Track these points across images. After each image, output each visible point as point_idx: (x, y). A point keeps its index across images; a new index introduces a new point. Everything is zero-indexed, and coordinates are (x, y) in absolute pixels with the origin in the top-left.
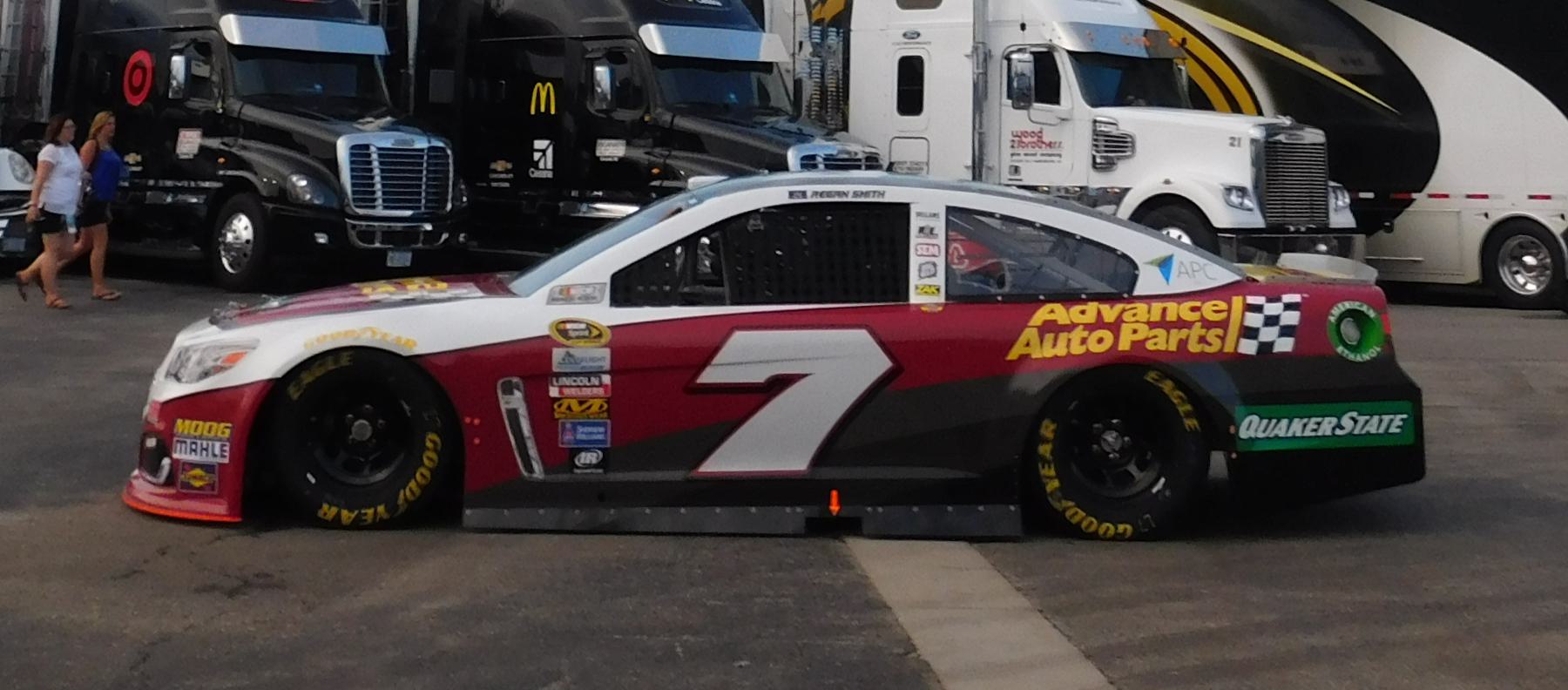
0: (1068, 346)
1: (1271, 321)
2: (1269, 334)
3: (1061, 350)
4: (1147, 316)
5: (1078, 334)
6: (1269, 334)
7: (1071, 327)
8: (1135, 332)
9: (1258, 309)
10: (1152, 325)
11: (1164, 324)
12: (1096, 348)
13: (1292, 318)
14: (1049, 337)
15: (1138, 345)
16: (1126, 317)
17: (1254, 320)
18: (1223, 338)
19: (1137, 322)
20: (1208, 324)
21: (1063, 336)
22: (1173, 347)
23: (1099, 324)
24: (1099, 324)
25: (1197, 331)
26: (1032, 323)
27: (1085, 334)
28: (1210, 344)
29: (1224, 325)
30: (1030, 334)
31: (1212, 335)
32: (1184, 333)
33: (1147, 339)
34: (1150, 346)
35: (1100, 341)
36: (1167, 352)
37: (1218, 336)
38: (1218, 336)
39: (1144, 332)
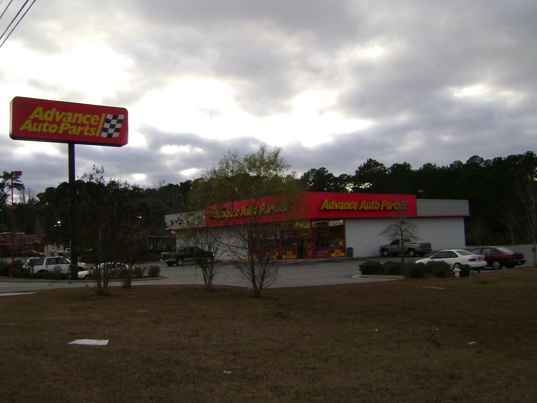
0: (42, 128)
1: (112, 126)
2: (111, 131)
3: (39, 130)
4: (71, 121)
5: (46, 125)
6: (111, 131)
7: (44, 122)
8: (65, 126)
9: (108, 121)
10: (72, 124)
11: (77, 125)
12: (51, 131)
14: (35, 124)
15: (65, 132)
16: (64, 120)
17: (107, 126)
18: (96, 131)
19: (67, 122)
20: (91, 126)
22: (78, 133)
23: (54, 122)
24: (54, 122)
25: (87, 128)
26: (30, 118)
27: (48, 125)
28: (91, 133)
29: (97, 126)
30: (29, 122)
31: (92, 130)
32: (83, 128)
33: (69, 130)
34: (70, 133)
35: (53, 129)
36: (76, 135)
39: (69, 126)
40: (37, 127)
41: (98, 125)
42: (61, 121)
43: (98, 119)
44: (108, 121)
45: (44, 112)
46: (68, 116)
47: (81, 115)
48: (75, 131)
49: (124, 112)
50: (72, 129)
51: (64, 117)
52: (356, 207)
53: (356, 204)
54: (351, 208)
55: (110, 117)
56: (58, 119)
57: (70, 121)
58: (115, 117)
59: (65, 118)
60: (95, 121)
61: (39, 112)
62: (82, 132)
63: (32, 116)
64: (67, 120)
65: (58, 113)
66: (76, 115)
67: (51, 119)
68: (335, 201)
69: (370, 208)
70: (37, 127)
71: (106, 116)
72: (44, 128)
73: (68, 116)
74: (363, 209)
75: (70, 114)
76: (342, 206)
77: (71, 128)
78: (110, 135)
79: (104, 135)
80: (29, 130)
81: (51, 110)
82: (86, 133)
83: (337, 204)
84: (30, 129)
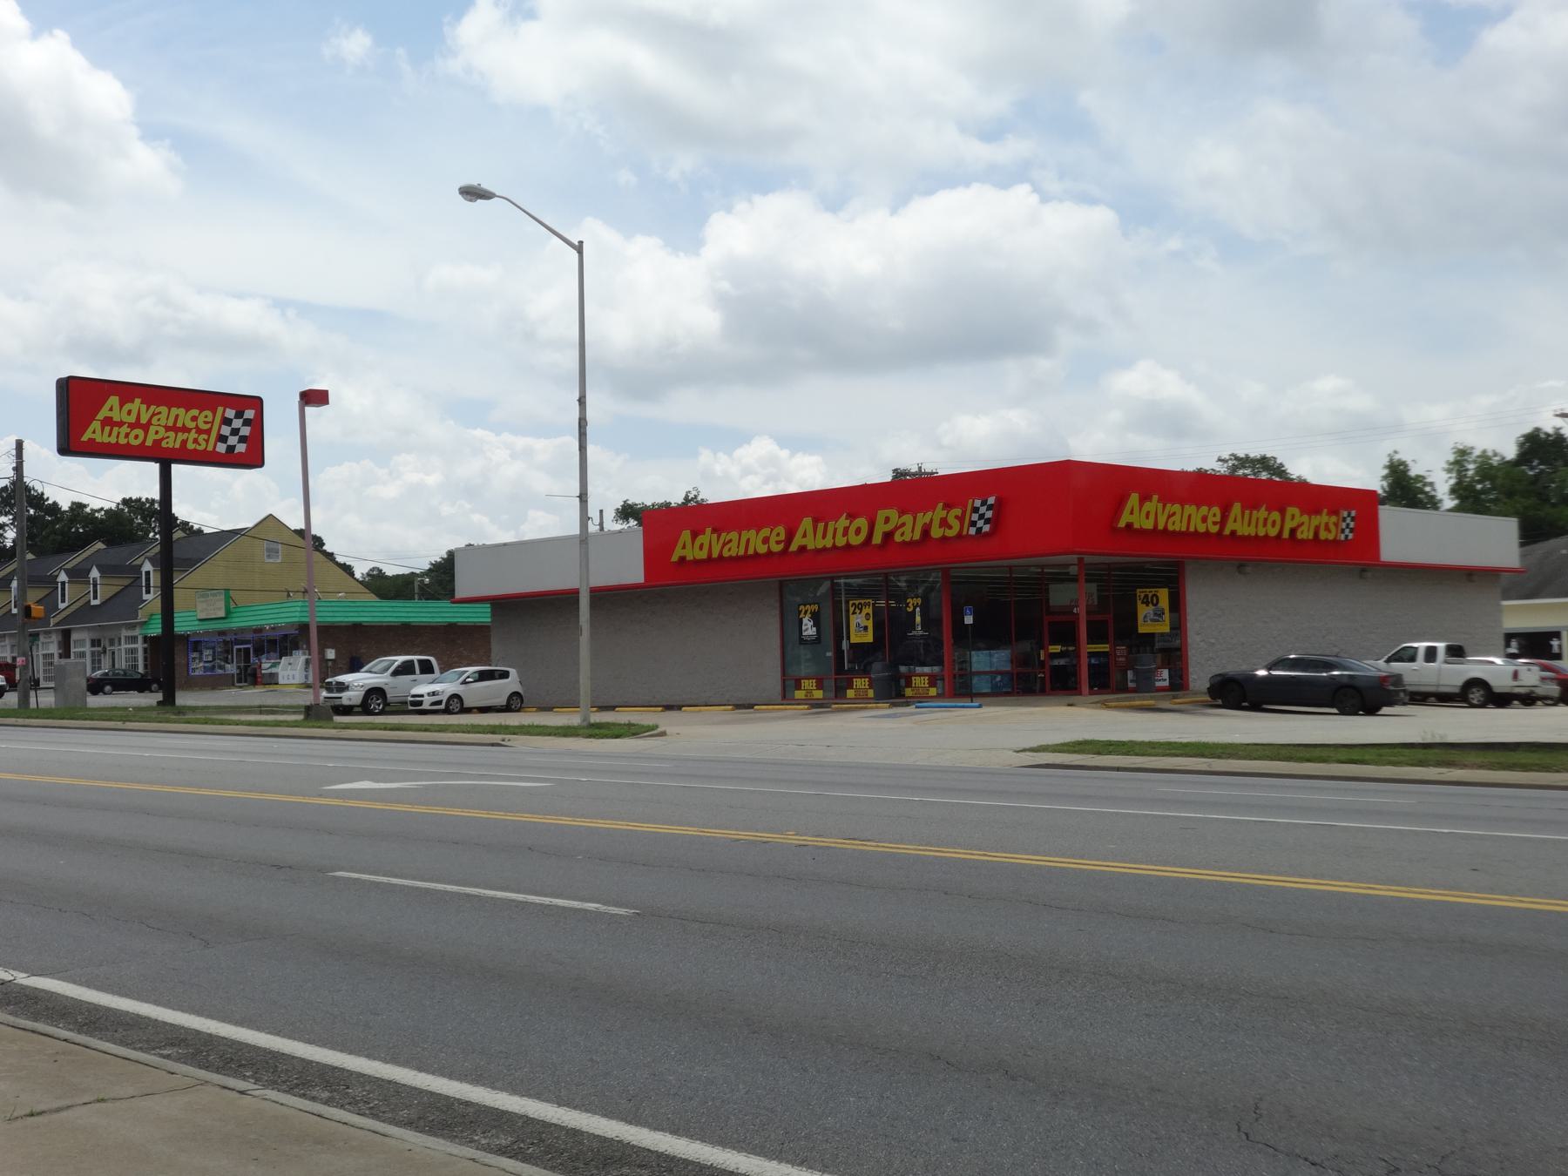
1: (235, 432)
2: (233, 440)
3: (113, 440)
5: (125, 429)
6: (233, 440)
7: (120, 424)
8: (157, 433)
9: (227, 422)
10: (168, 429)
11: (174, 429)
12: (135, 443)
14: (107, 429)
15: (157, 442)
17: (226, 430)
18: (207, 441)
19: (159, 425)
20: (199, 431)
21: (116, 429)
22: (177, 445)
25: (193, 435)
28: (200, 445)
29: (208, 432)
30: (96, 425)
33: (163, 439)
34: (164, 444)
36: (173, 449)
37: (204, 439)
38: (204, 439)
40: (110, 435)
41: (211, 428)
42: (149, 423)
43: (210, 419)
44: (227, 422)
45: (121, 405)
46: (160, 413)
47: (181, 411)
48: (172, 442)
49: (256, 403)
50: (168, 437)
51: (154, 414)
52: (778, 543)
53: (778, 534)
54: (762, 549)
55: (230, 413)
56: (144, 420)
57: (163, 422)
58: (239, 415)
59: (155, 418)
60: (206, 423)
61: (112, 407)
62: (184, 442)
63: (101, 416)
64: (159, 420)
65: (144, 407)
66: (174, 411)
67: (132, 419)
68: (1158, 502)
69: (828, 543)
70: (110, 435)
71: (224, 412)
72: (119, 436)
73: (160, 413)
74: (803, 549)
75: (164, 409)
76: (734, 545)
77: (167, 435)
78: (231, 449)
79: (221, 448)
80: (97, 441)
81: (133, 402)
82: (191, 446)
83: (718, 540)
84: (98, 438)
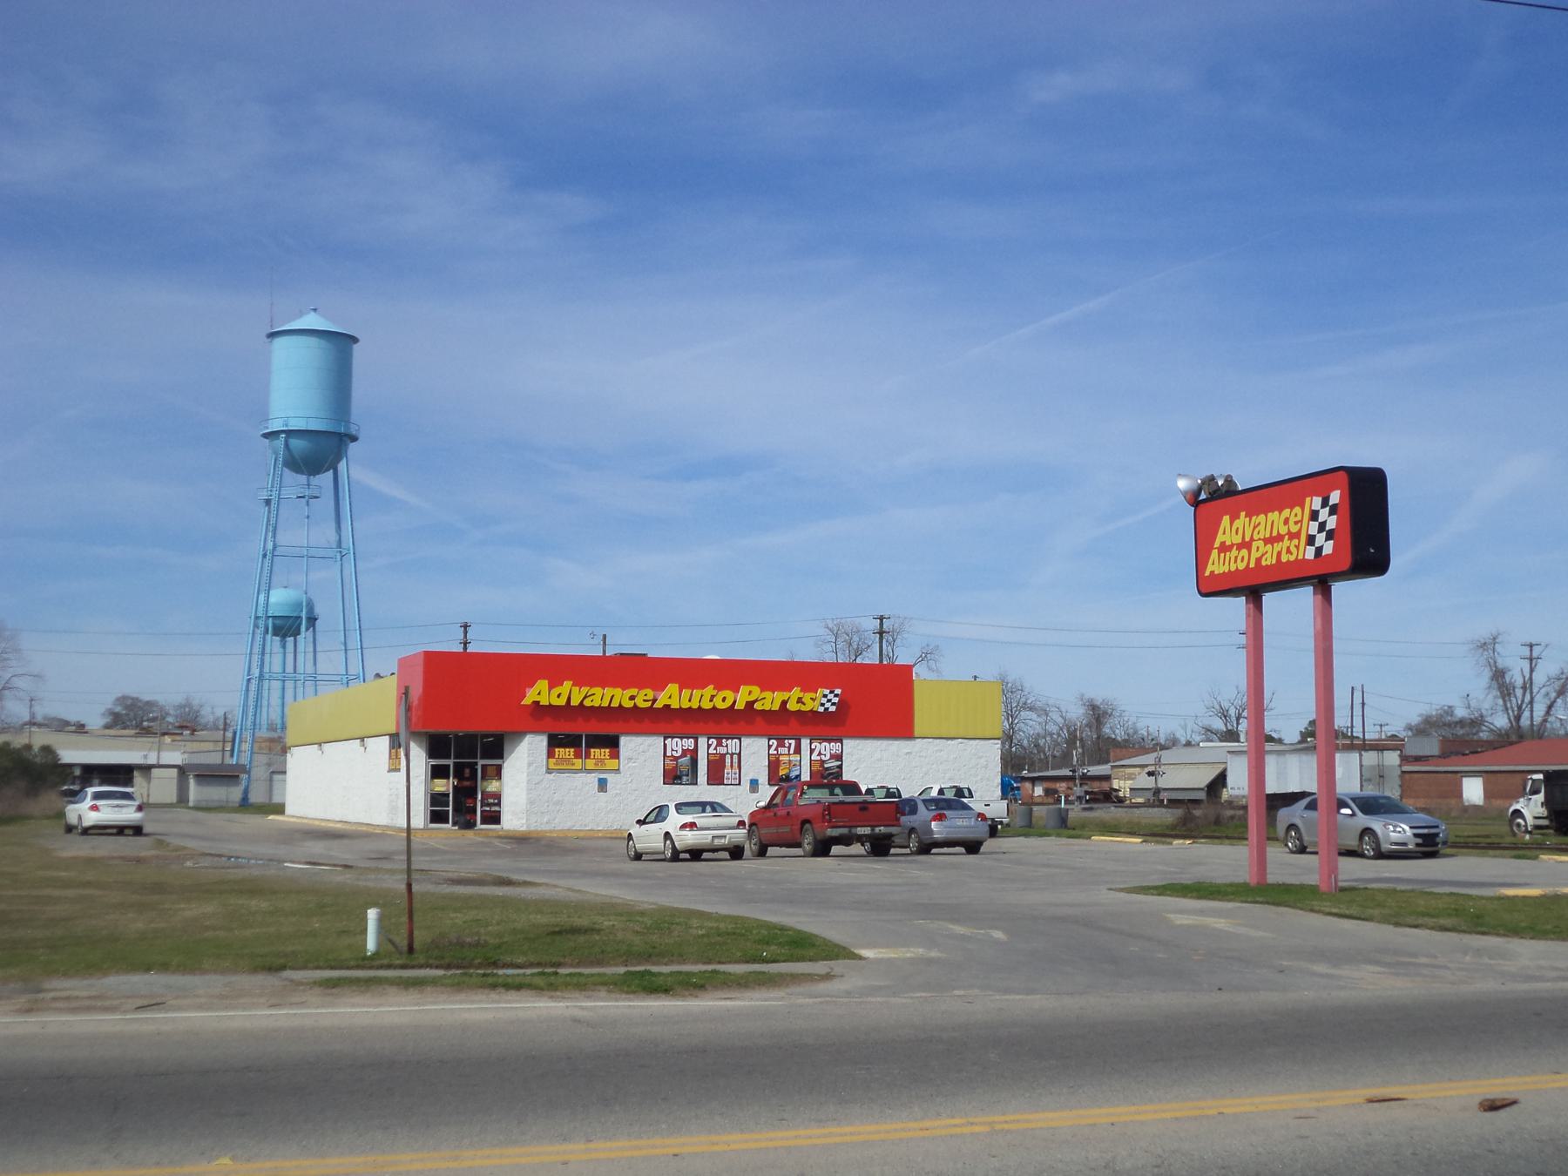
1: (829, 701)
8: (750, 693)
9: (825, 696)
13: (836, 700)
17: (824, 700)
22: (776, 707)
44: (825, 696)
58: (831, 692)
